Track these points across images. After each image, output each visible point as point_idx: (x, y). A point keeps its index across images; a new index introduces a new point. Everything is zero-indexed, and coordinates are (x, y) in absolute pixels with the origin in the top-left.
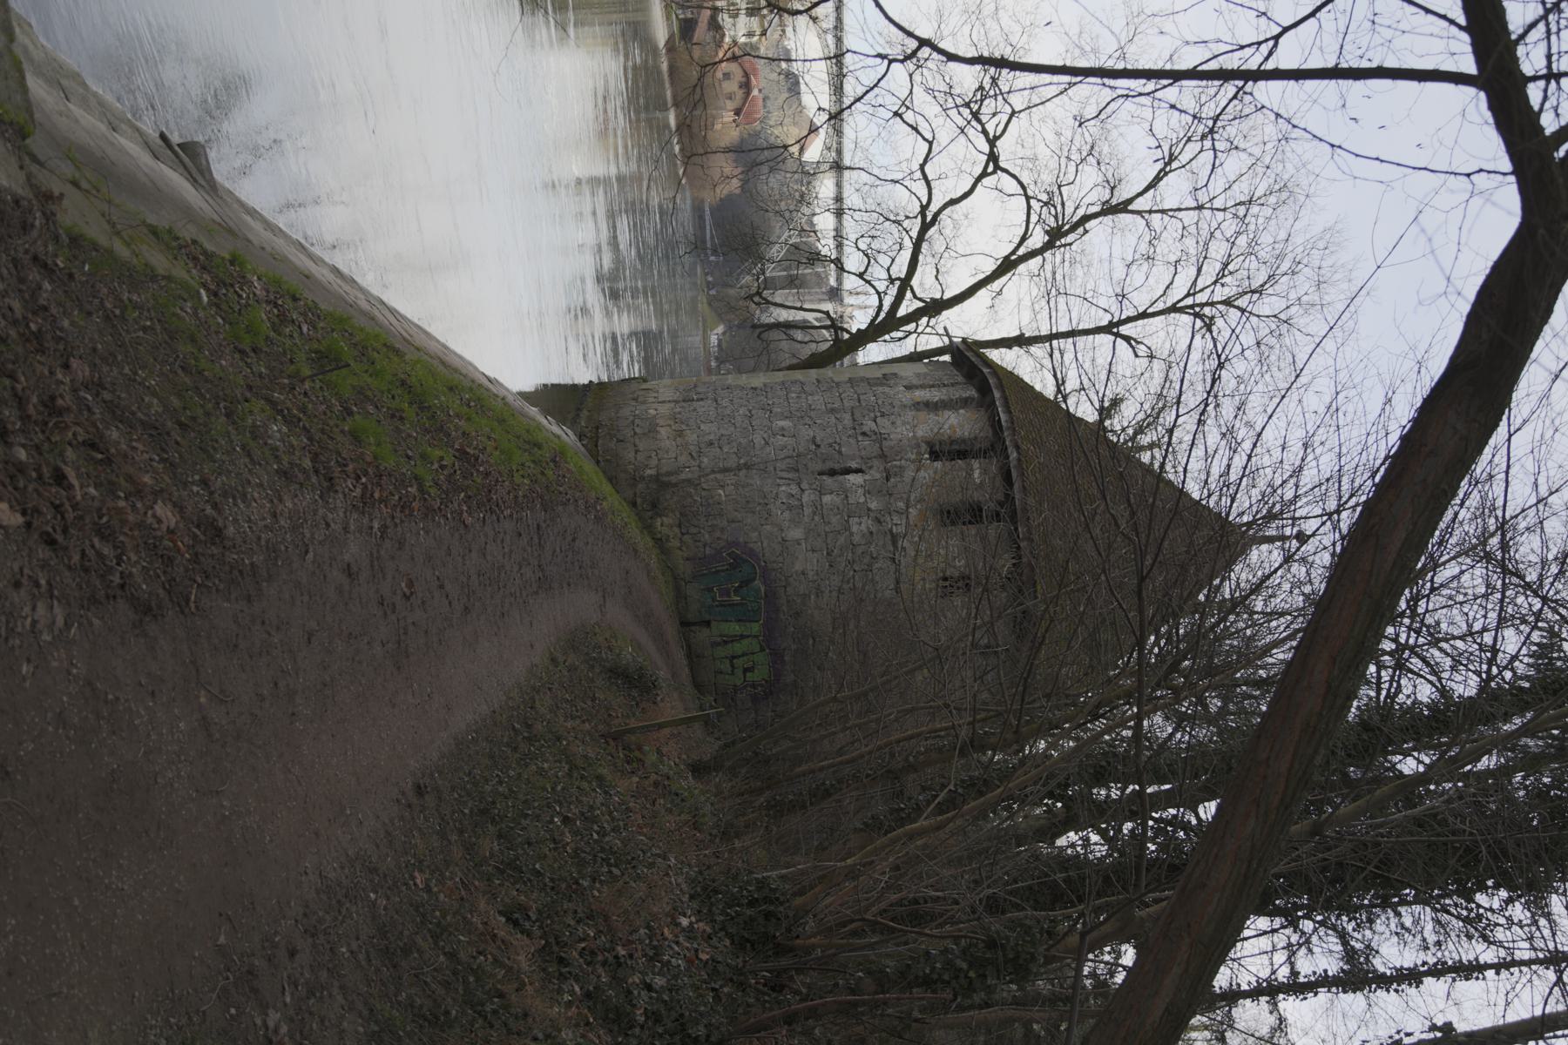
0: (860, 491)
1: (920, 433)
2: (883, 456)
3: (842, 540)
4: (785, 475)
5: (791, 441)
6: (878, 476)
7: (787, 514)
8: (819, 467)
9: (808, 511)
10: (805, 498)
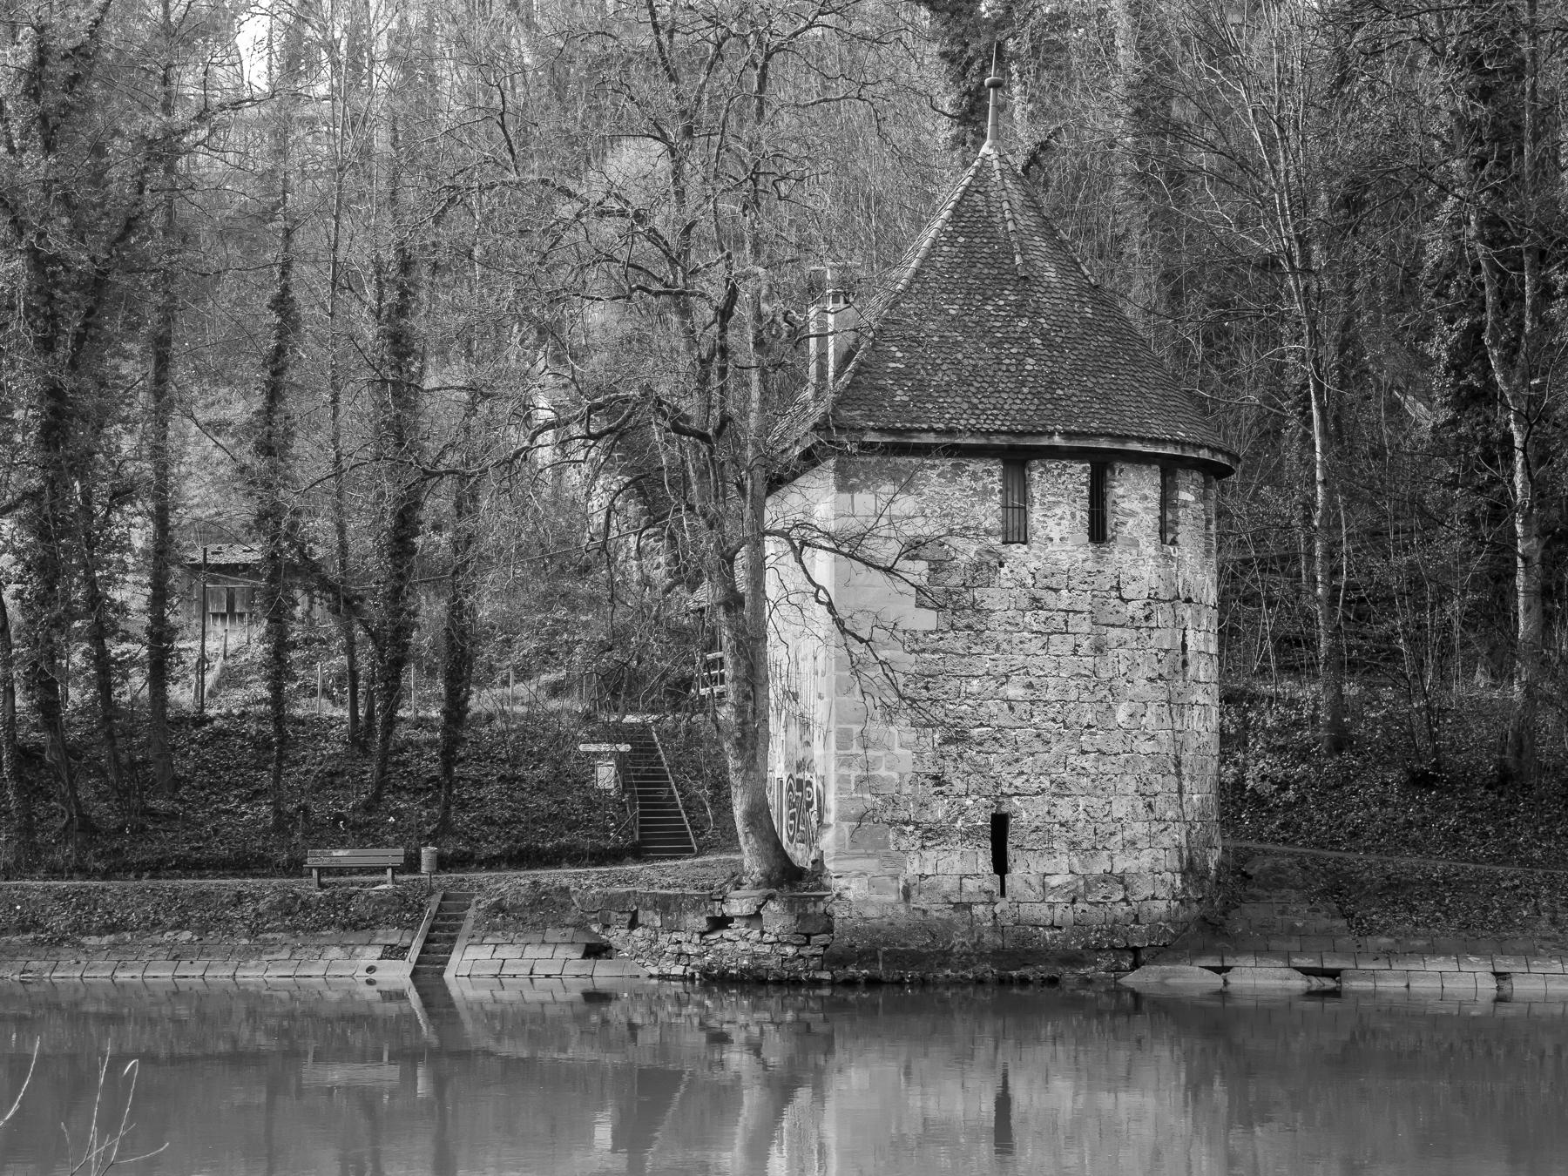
1: (1152, 551)
5: (1153, 708)
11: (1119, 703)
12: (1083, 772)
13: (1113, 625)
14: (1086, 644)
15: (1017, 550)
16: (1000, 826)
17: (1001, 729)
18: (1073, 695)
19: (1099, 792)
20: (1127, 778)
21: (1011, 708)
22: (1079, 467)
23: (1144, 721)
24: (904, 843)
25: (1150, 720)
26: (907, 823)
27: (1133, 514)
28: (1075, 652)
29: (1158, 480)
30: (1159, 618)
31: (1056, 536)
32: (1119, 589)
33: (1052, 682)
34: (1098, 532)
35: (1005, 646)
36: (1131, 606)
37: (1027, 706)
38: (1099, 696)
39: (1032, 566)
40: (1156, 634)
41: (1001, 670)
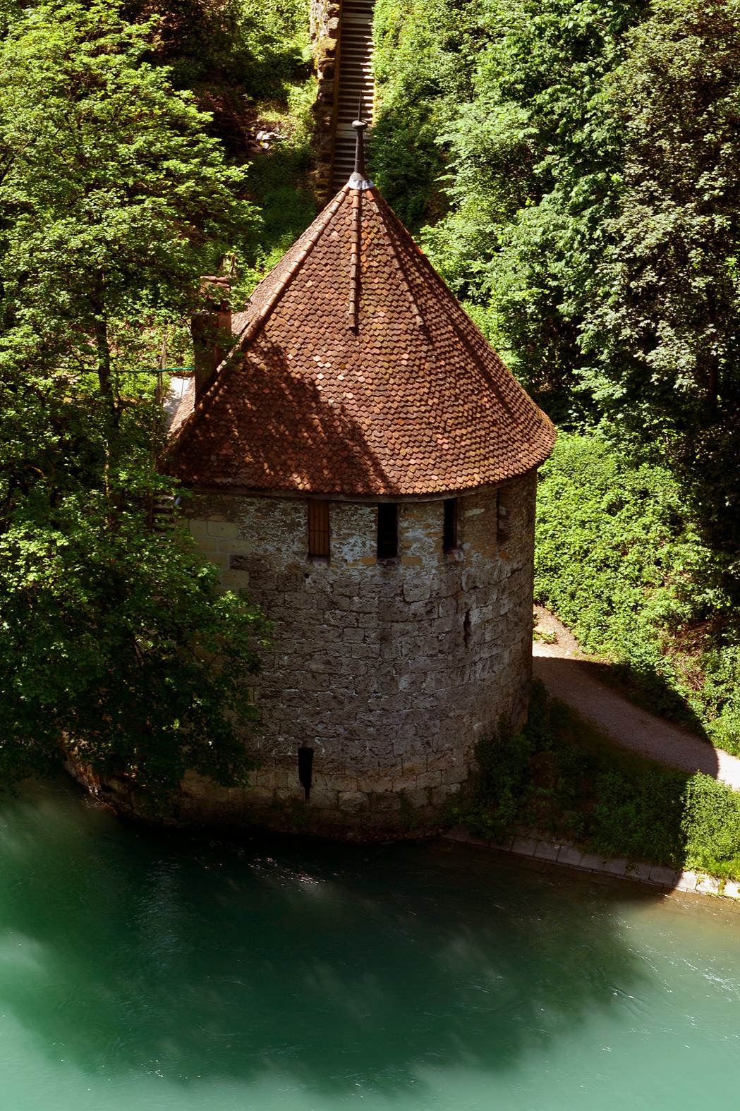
0: (485, 610)
1: (435, 563)
4: (466, 678)
6: (474, 597)
8: (462, 649)
9: (495, 651)
10: (485, 655)
11: (401, 675)
13: (397, 622)
14: (373, 636)
15: (319, 566)
17: (306, 691)
18: (363, 670)
19: (383, 738)
20: (407, 727)
21: (314, 677)
22: (368, 510)
23: (424, 685)
25: (429, 684)
27: (417, 540)
31: (349, 557)
32: (402, 594)
33: (344, 660)
35: (309, 634)
36: (413, 607)
38: (384, 671)
39: (331, 578)
40: (437, 623)
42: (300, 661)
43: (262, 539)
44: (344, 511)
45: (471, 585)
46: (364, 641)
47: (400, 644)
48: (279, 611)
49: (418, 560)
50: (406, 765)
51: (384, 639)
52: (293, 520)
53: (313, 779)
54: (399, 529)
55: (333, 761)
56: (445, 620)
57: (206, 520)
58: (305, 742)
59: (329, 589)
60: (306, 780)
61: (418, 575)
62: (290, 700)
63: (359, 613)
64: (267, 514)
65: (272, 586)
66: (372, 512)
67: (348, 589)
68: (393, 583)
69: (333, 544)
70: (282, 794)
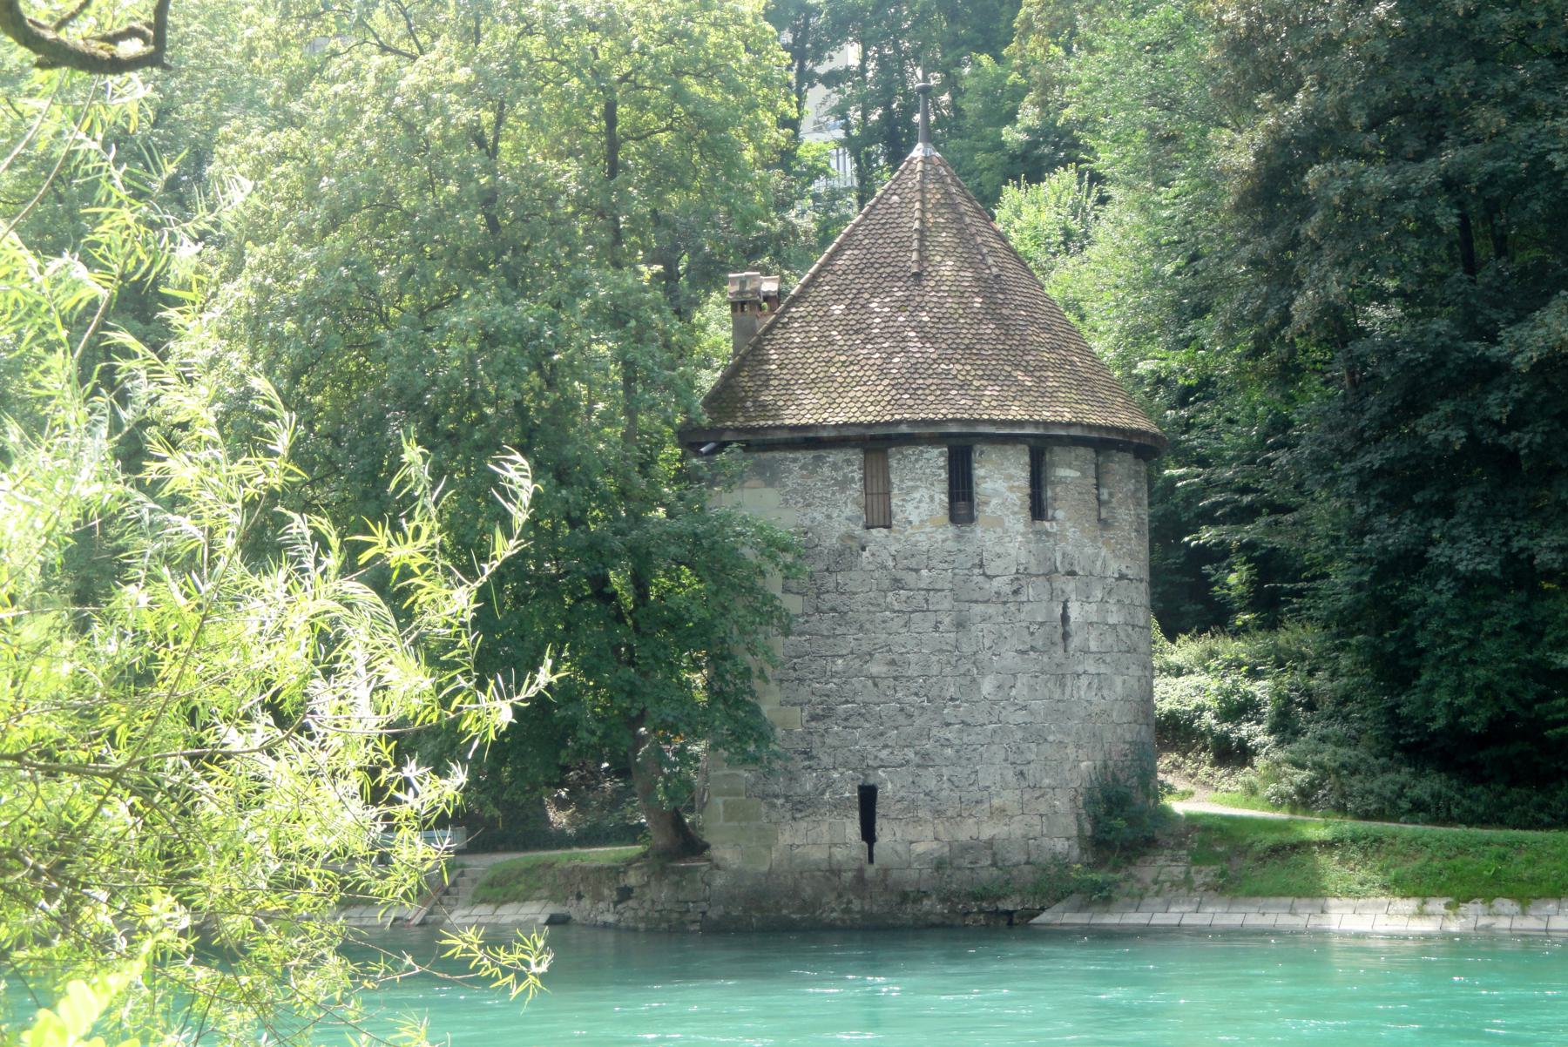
0: (1087, 607)
1: (1021, 527)
2: (1050, 574)
3: (1122, 635)
5: (1022, 680)
7: (1105, 692)
8: (1060, 652)
11: (983, 675)
12: (948, 743)
13: (976, 602)
14: (947, 620)
15: (878, 533)
16: (868, 798)
17: (866, 704)
18: (935, 670)
19: (964, 762)
20: (994, 748)
21: (876, 685)
22: (936, 452)
23: (1013, 693)
24: (774, 816)
25: (1020, 691)
26: (777, 796)
27: (996, 493)
28: (936, 629)
29: (1027, 459)
30: (1029, 592)
31: (914, 518)
32: (981, 566)
33: (912, 657)
34: (1038, 509)
35: (868, 626)
36: (996, 583)
37: (892, 682)
39: (892, 549)
40: (1027, 608)
41: (865, 648)
42: (857, 663)
43: (809, 505)
44: (905, 457)
45: (1068, 568)
46: (936, 629)
47: (982, 633)
48: (831, 599)
49: (999, 521)
50: (996, 802)
51: (960, 625)
52: (845, 476)
53: (877, 828)
54: (975, 479)
55: (902, 799)
56: (1037, 607)
57: (741, 487)
58: (866, 776)
59: (891, 563)
60: (868, 834)
61: (1000, 540)
62: (846, 720)
63: (928, 590)
64: (814, 472)
65: (822, 566)
66: (941, 454)
67: (912, 560)
68: (970, 549)
69: (894, 501)
70: (839, 854)
